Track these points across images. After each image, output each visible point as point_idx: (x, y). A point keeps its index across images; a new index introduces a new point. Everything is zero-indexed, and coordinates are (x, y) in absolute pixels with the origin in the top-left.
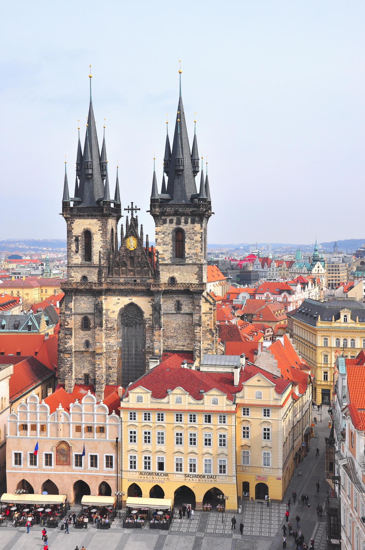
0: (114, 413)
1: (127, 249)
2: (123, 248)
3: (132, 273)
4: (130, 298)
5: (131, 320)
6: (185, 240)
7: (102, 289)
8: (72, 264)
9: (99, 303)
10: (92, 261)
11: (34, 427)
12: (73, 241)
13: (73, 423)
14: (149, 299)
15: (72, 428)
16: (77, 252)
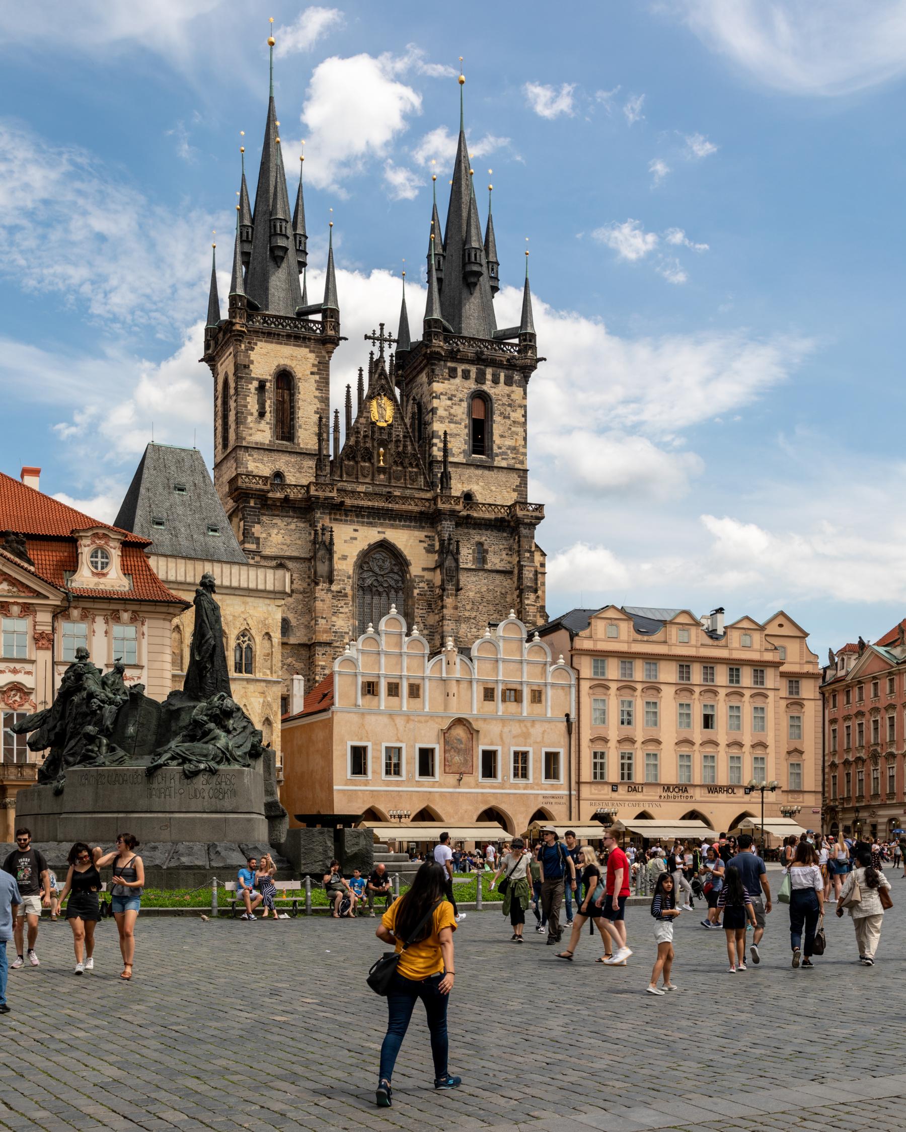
0: (561, 661)
1: (374, 423)
2: (362, 420)
3: (382, 476)
4: (380, 529)
5: (380, 579)
6: (492, 417)
7: (333, 498)
8: (249, 443)
9: (323, 529)
10: (296, 441)
11: (394, 689)
12: (253, 390)
13: (478, 681)
14: (421, 535)
15: (478, 692)
16: (262, 414)
